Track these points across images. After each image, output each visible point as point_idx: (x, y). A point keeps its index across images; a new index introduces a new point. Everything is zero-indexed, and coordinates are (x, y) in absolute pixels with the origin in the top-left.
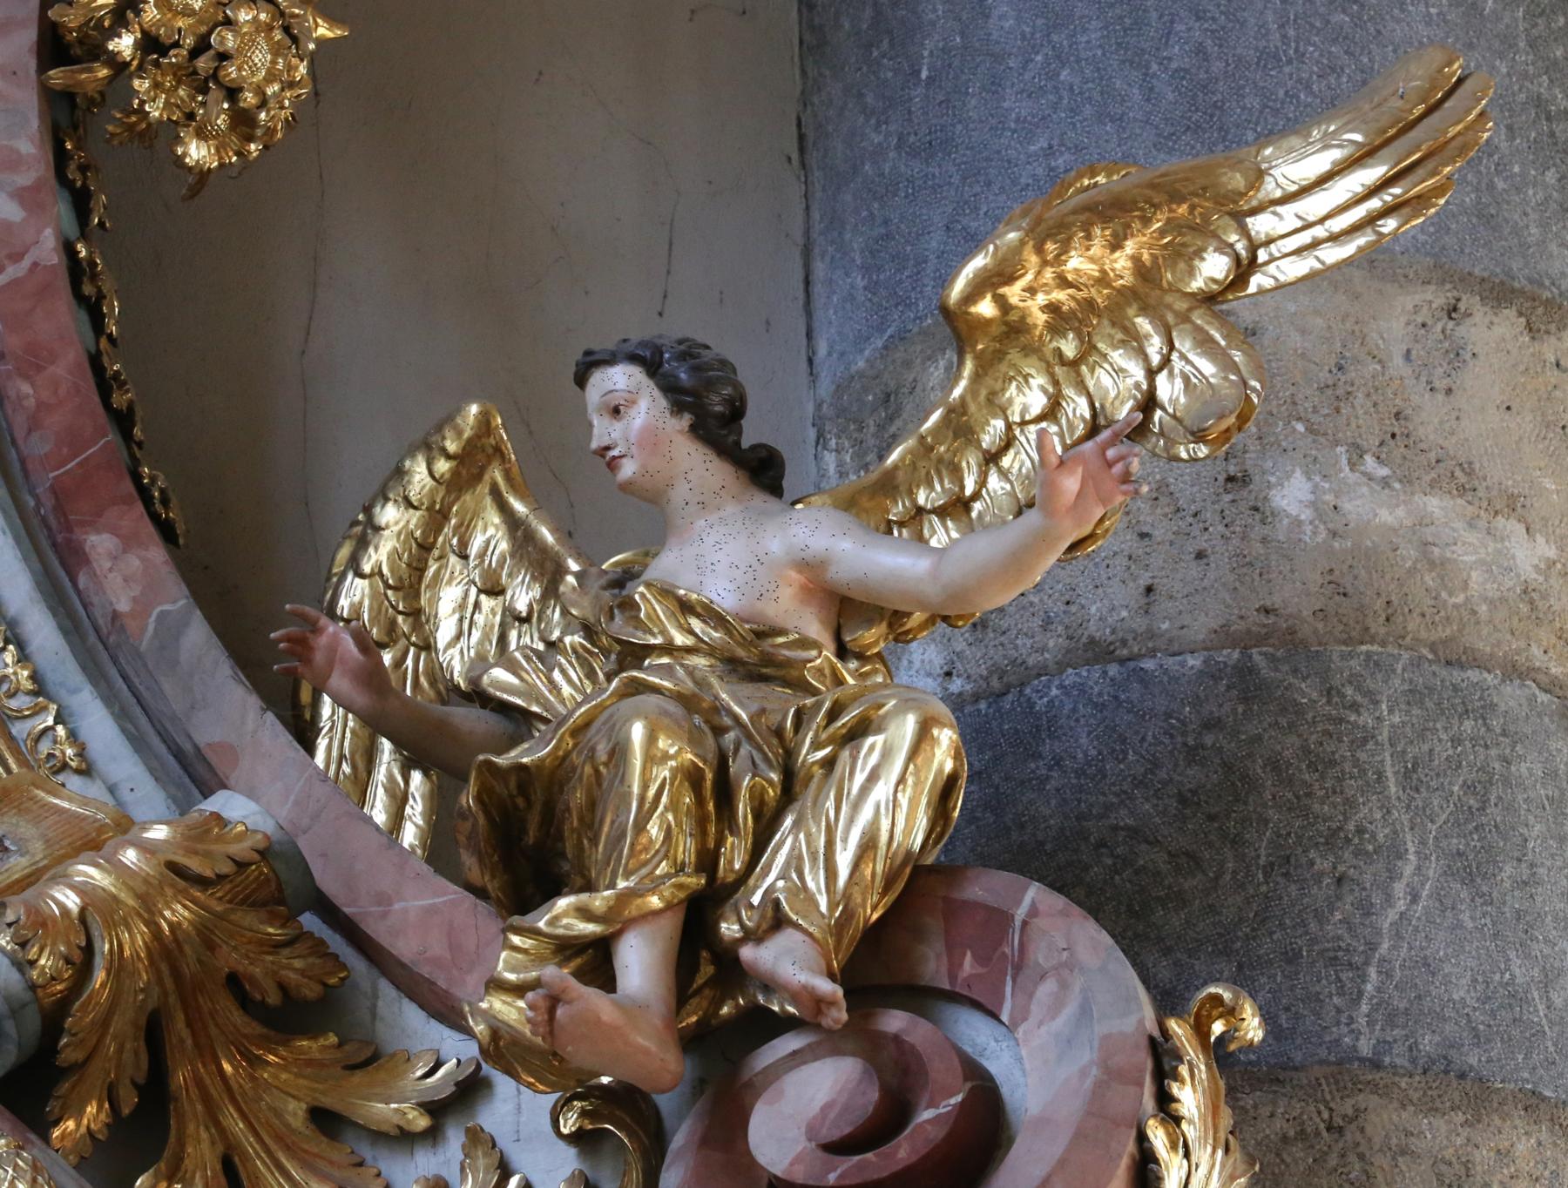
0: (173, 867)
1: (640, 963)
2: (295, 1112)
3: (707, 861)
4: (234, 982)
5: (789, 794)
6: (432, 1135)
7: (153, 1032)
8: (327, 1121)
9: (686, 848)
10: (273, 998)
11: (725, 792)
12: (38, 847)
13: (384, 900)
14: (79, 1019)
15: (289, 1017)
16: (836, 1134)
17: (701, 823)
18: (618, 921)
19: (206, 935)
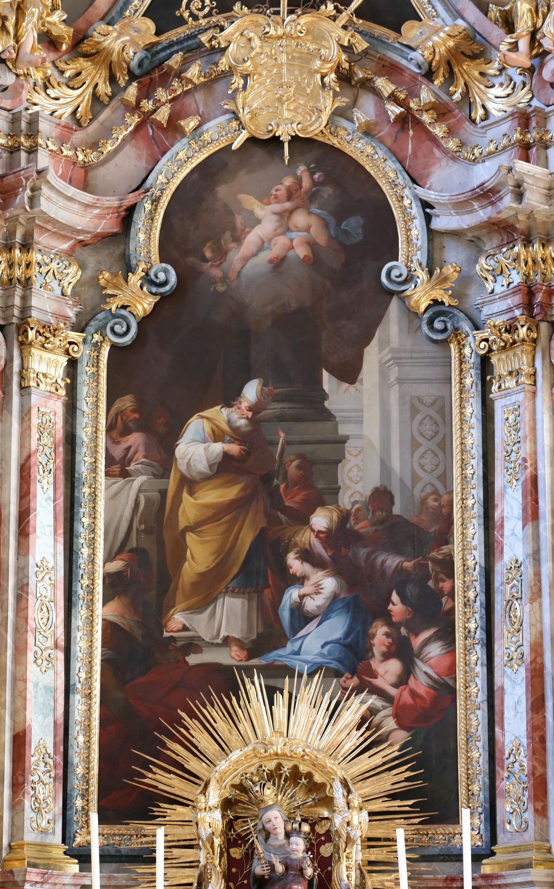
0: (449, 35)
1: (523, 44)
2: (476, 74)
3: (534, 25)
4: (462, 53)
5: (549, 10)
6: (501, 74)
7: (449, 63)
8: (482, 74)
9: (530, 24)
10: (471, 54)
11: (537, 11)
12: (428, 33)
13: (490, 33)
14: (434, 64)
15: (474, 57)
16: (275, 211)
17: (533, 18)
18: (518, 38)
19: (457, 46)
